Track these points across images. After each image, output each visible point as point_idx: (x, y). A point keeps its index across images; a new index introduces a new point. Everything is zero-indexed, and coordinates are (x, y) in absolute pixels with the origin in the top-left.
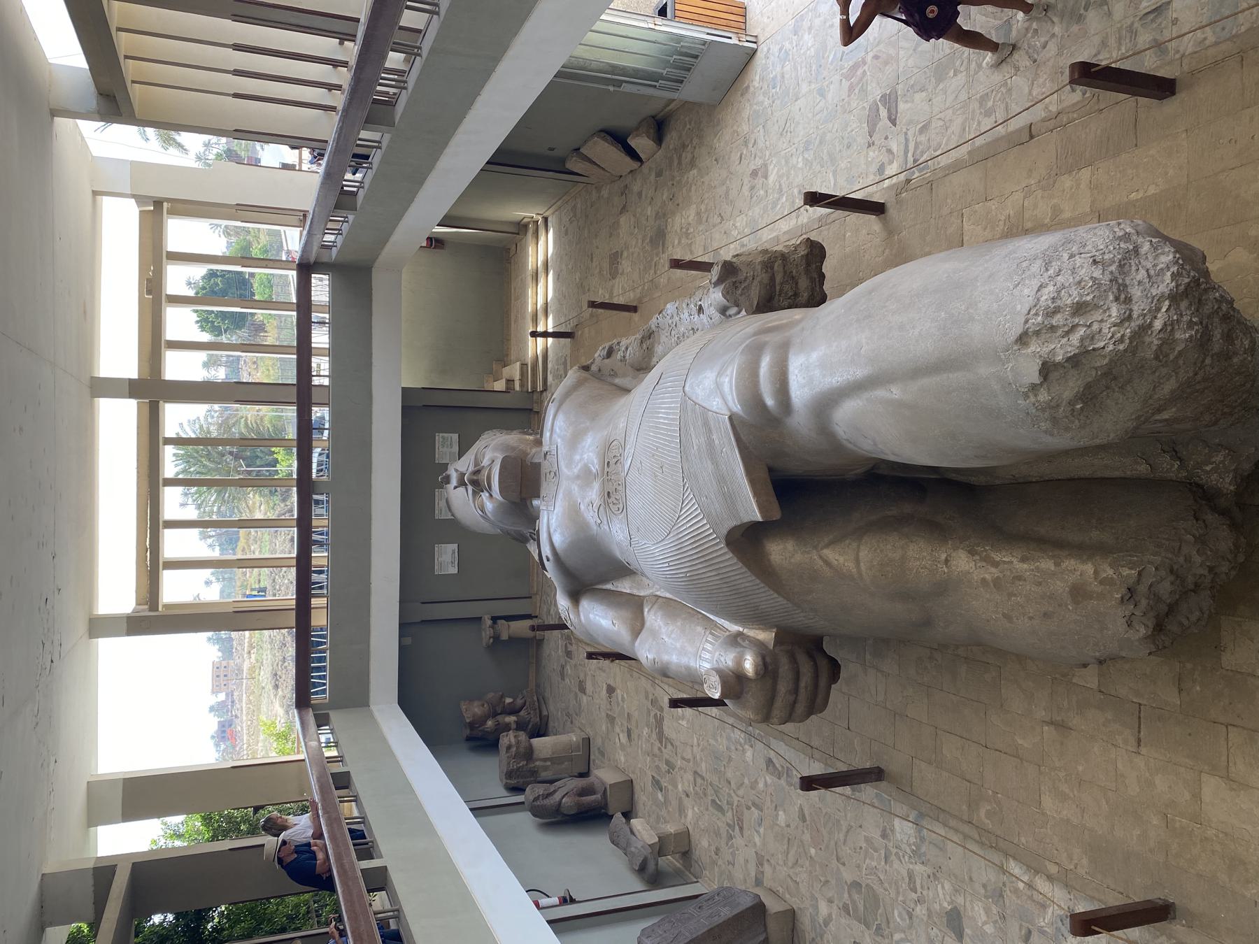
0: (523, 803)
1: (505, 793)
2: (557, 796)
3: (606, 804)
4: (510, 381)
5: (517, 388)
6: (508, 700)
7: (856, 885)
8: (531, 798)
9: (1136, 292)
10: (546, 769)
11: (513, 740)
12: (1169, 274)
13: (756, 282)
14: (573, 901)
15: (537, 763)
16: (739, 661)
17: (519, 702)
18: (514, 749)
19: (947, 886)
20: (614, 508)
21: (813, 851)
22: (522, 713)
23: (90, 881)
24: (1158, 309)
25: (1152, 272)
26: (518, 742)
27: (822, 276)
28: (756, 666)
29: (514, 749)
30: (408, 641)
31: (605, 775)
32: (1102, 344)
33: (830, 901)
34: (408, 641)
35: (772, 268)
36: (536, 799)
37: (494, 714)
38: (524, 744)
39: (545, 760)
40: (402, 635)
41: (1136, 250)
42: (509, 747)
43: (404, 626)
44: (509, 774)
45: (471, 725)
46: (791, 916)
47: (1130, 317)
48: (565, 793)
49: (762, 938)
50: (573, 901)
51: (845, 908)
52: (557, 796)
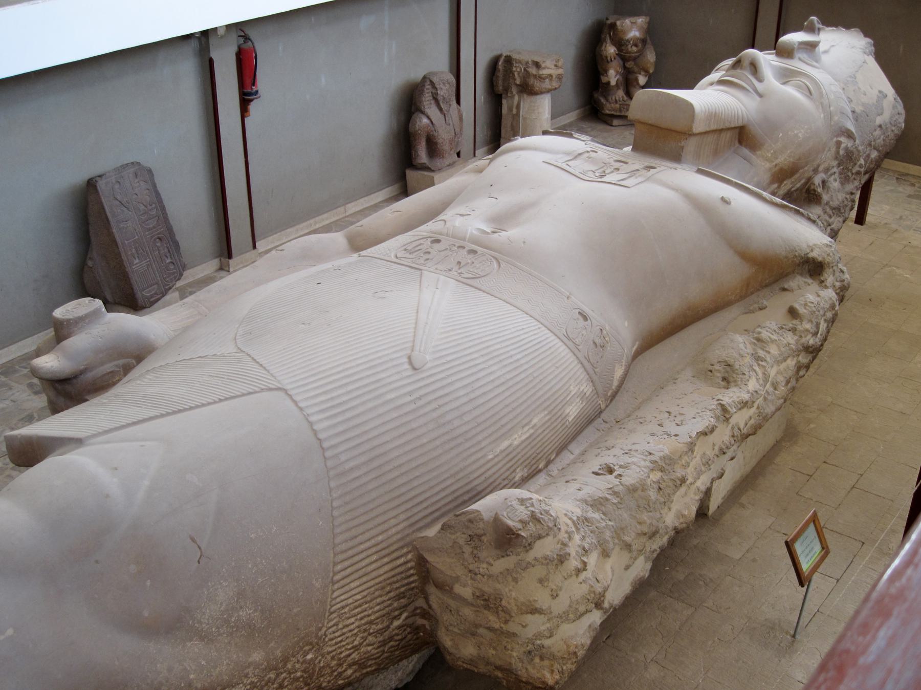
2: (432, 110)
10: (510, 109)
11: (545, 72)
13: (460, 571)
15: (516, 98)
22: (620, 93)
26: (541, 78)
29: (533, 70)
35: (487, 607)
36: (432, 83)
37: (623, 57)
38: (537, 85)
39: (518, 107)
44: (509, 60)
45: (613, 26)
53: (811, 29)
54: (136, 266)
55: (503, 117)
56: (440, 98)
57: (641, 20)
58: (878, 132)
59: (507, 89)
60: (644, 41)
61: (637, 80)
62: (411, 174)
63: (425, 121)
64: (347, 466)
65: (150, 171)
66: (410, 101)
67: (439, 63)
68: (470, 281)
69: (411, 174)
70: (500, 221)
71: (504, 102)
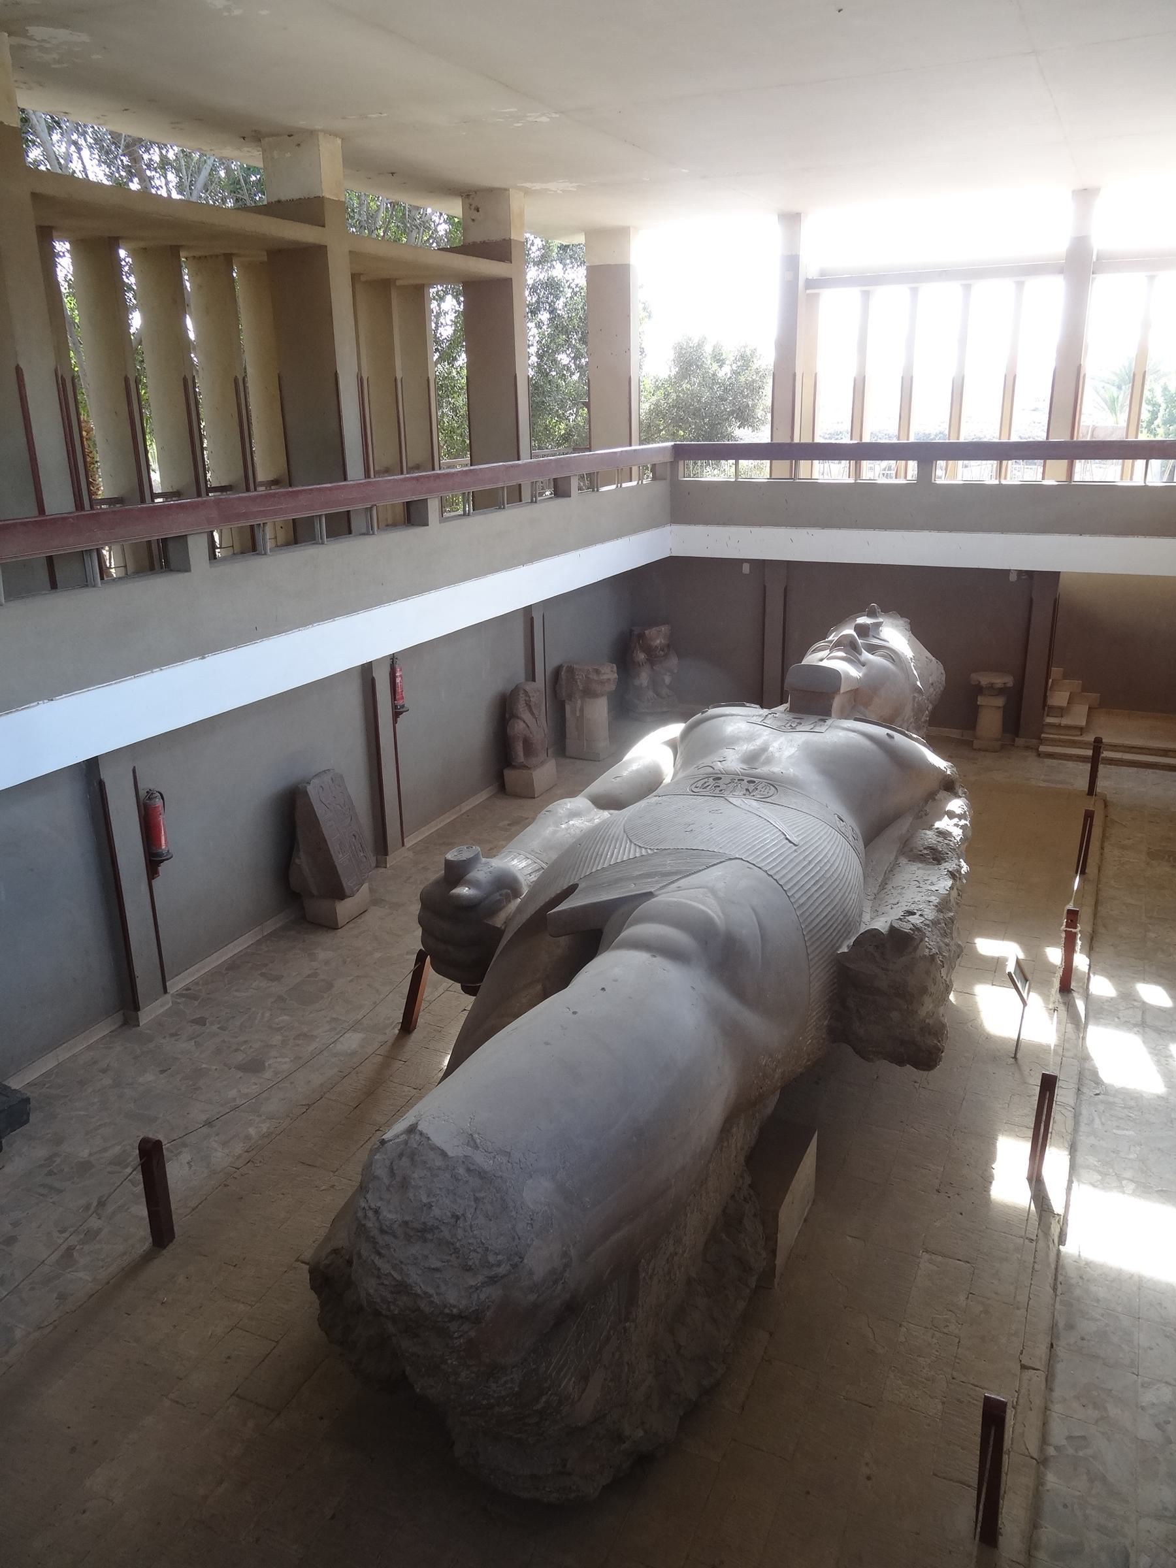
0: (534, 680)
1: (552, 664)
2: (526, 716)
3: (515, 767)
4: (1061, 711)
5: (1049, 720)
6: (668, 679)
7: (330, 986)
8: (527, 688)
9: (416, 1249)
11: (605, 677)
12: (431, 1291)
14: (397, 714)
15: (579, 702)
16: (470, 884)
17: (664, 691)
18: (595, 677)
19: (285, 1067)
20: (700, 784)
21: (377, 955)
22: (651, 693)
23: (495, 237)
24: (394, 1267)
25: (437, 1275)
26: (602, 683)
27: (901, 1062)
28: (459, 897)
29: (595, 677)
30: (746, 568)
31: (544, 772)
32: (369, 1196)
33: (327, 963)
34: (746, 568)
39: (582, 710)
40: (753, 563)
41: (468, 1269)
42: (597, 672)
43: (760, 565)
45: (642, 636)
46: (331, 925)
47: (382, 1231)
48: (533, 724)
49: (315, 892)
50: (397, 714)
51: (315, 975)
52: (526, 716)
53: (872, 614)
54: (341, 860)
55: (567, 724)
56: (532, 704)
57: (664, 629)
58: (931, 690)
59: (570, 696)
60: (669, 646)
61: (663, 681)
62: (509, 774)
63: (522, 725)
64: (801, 901)
65: (342, 777)
66: (505, 710)
67: (521, 676)
68: (763, 800)
69: (509, 774)
70: (752, 758)
71: (568, 708)
